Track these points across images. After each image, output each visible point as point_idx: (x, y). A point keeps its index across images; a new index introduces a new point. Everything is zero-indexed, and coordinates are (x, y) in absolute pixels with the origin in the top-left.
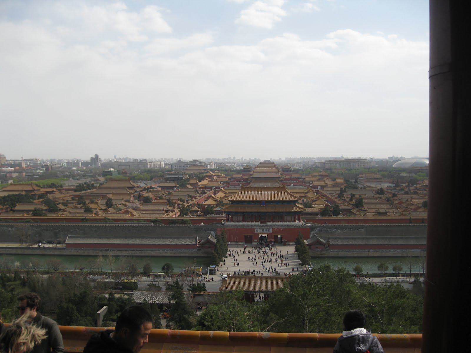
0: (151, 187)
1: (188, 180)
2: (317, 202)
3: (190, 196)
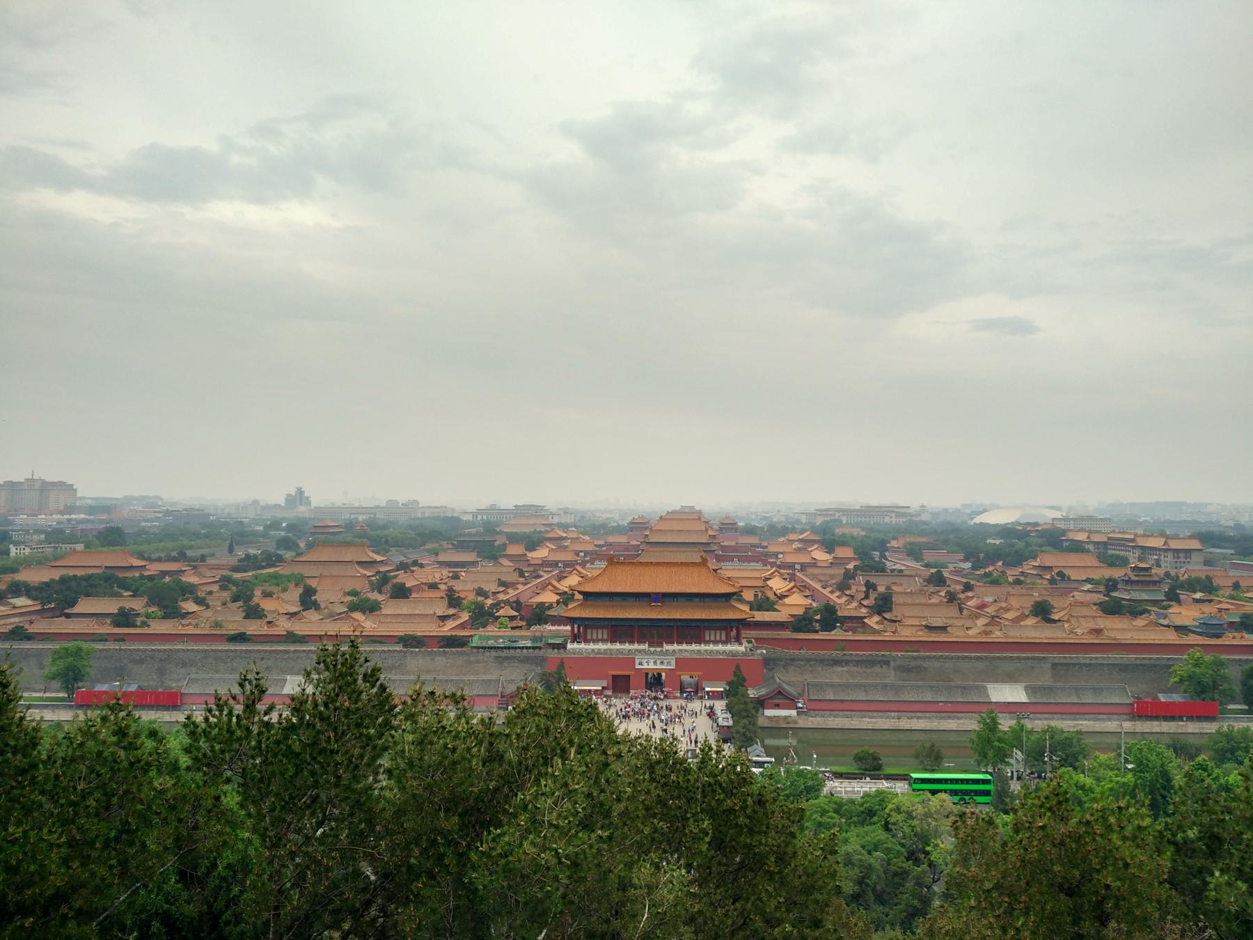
1: (504, 546)
2: (787, 601)
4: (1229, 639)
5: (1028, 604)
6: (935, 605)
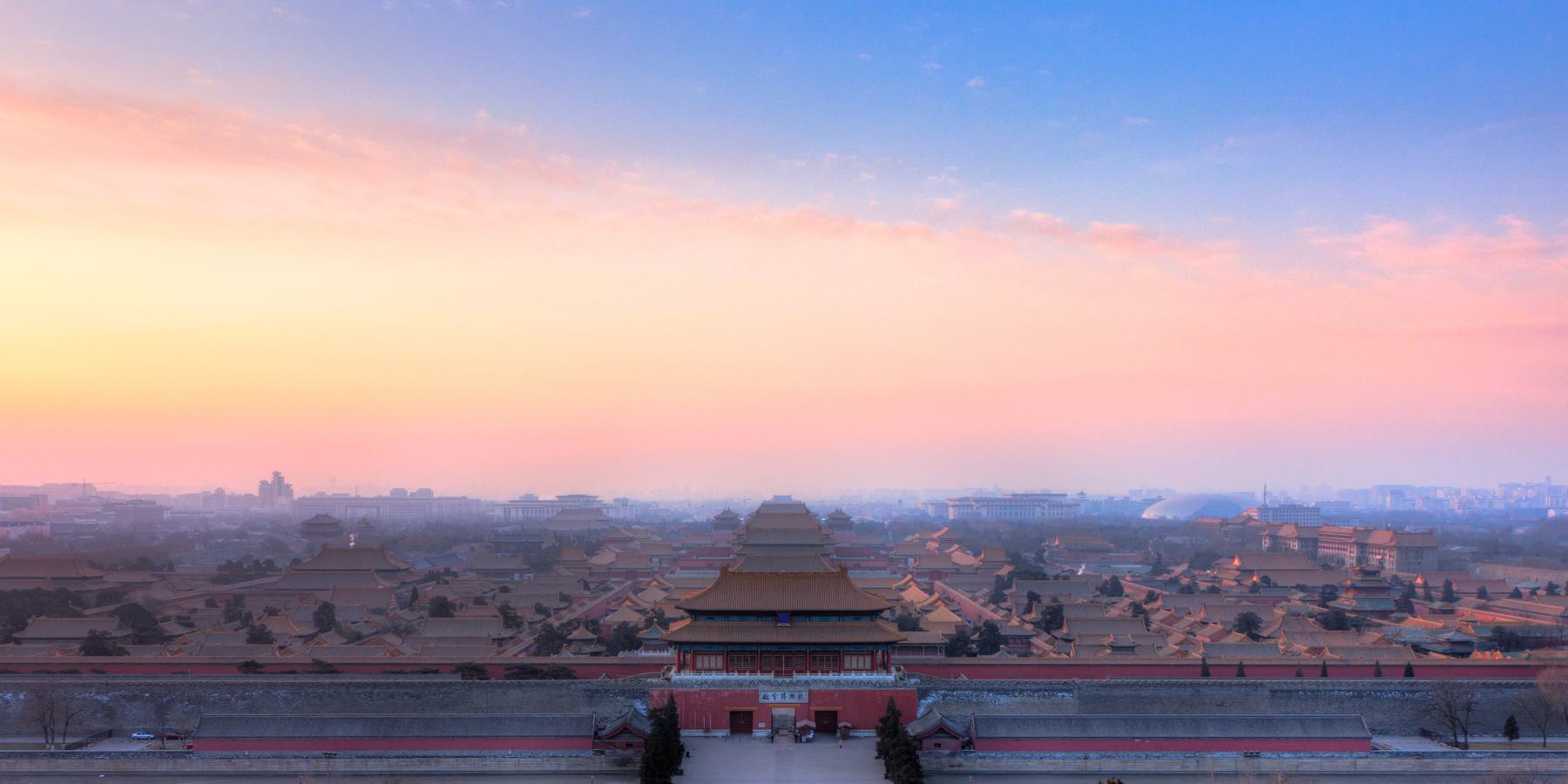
0: (448, 571)
2: (931, 617)
3: (564, 598)
4: (1478, 657)
5: (1232, 617)
6: (1112, 620)
